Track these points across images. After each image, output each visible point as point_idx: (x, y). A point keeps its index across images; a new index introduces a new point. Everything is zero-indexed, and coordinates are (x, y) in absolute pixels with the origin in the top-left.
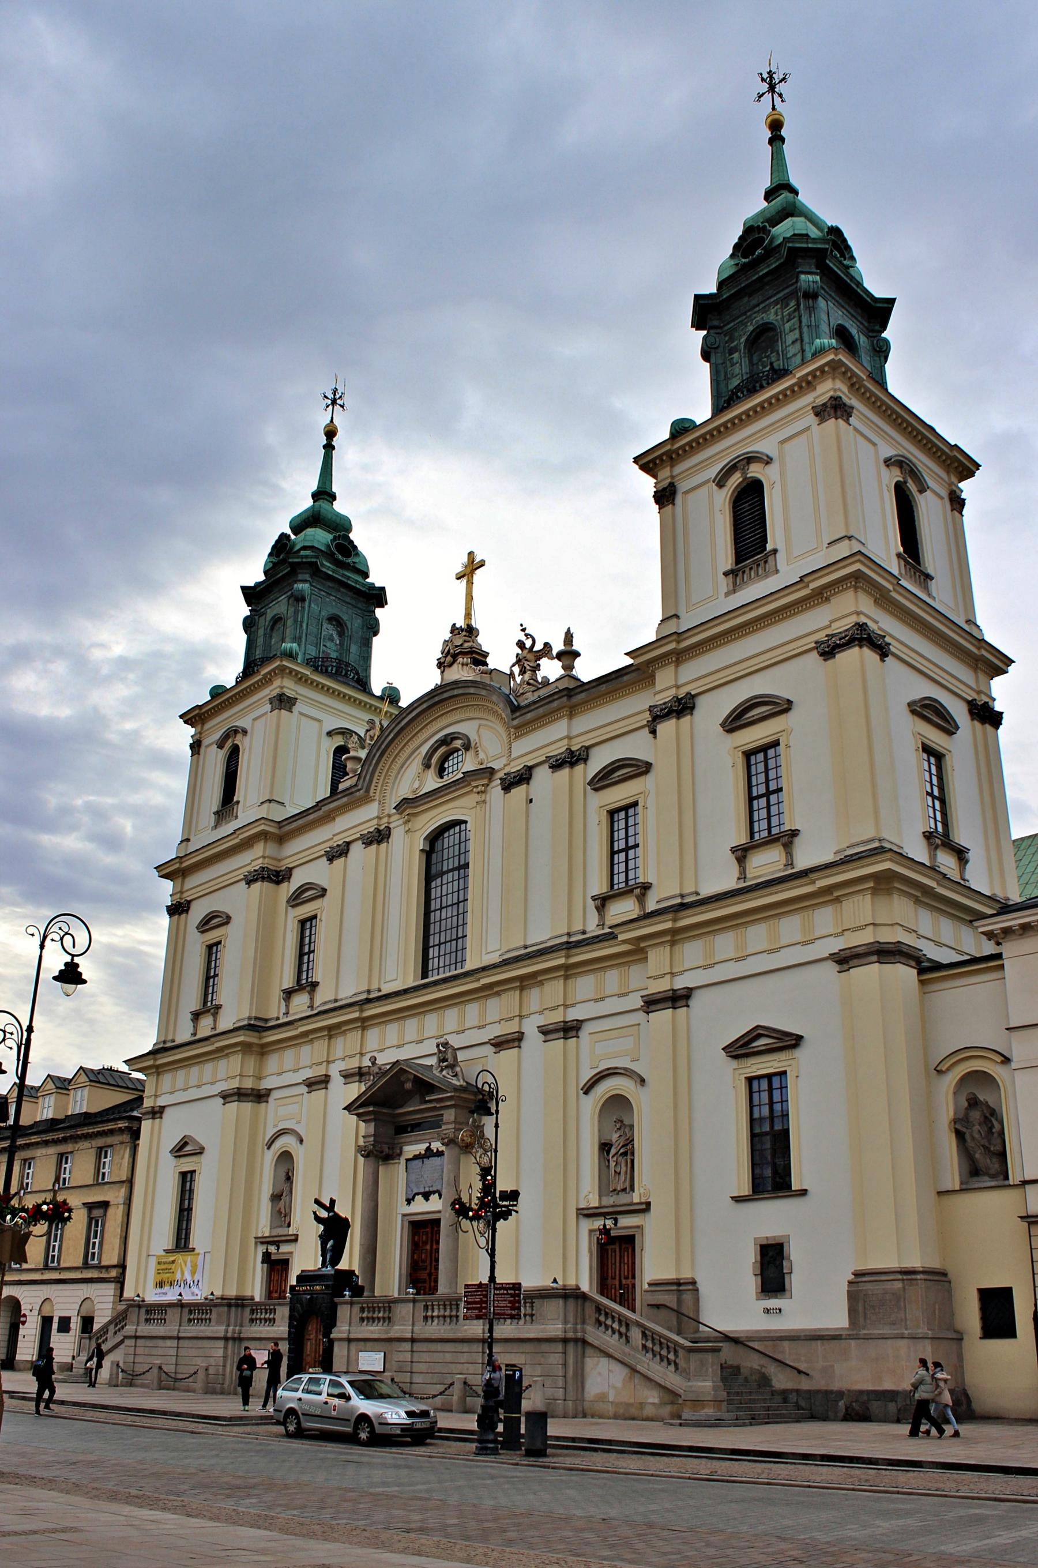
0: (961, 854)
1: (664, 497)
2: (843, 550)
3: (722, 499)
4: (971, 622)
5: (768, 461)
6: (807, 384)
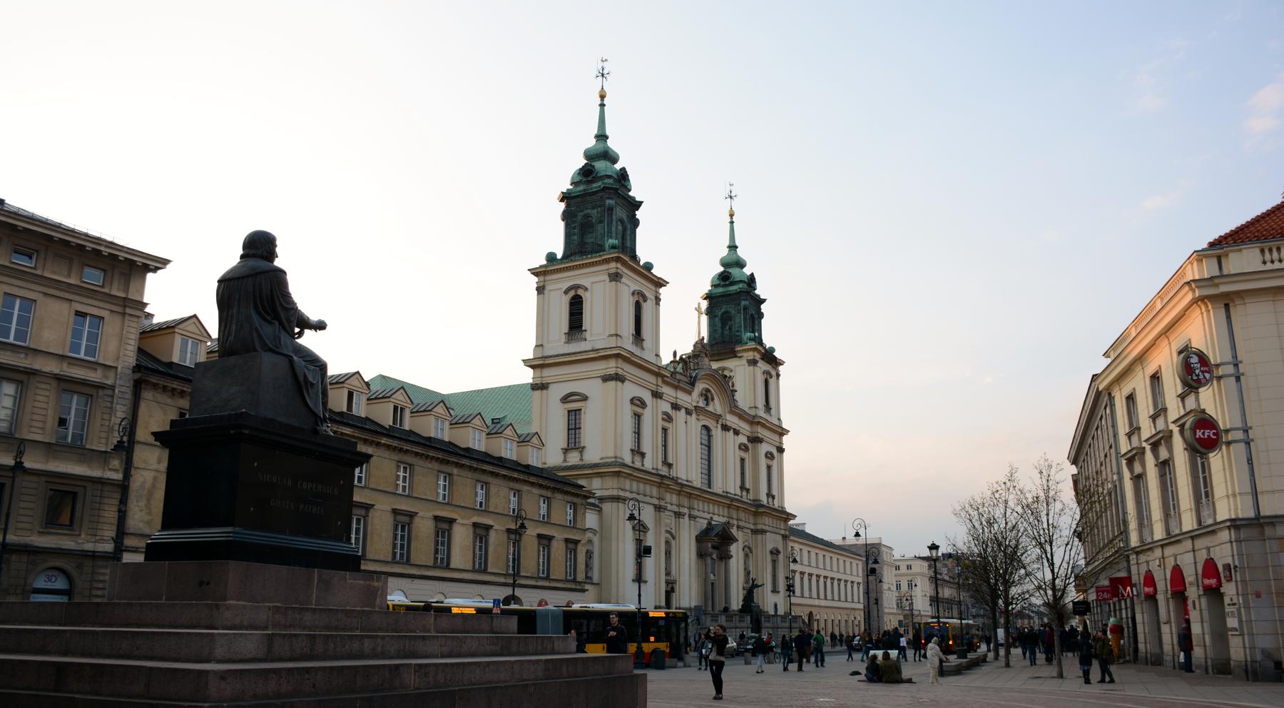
0: (643, 455)
1: (540, 290)
2: (612, 342)
3: (566, 300)
4: (657, 355)
5: (586, 289)
6: (607, 261)
